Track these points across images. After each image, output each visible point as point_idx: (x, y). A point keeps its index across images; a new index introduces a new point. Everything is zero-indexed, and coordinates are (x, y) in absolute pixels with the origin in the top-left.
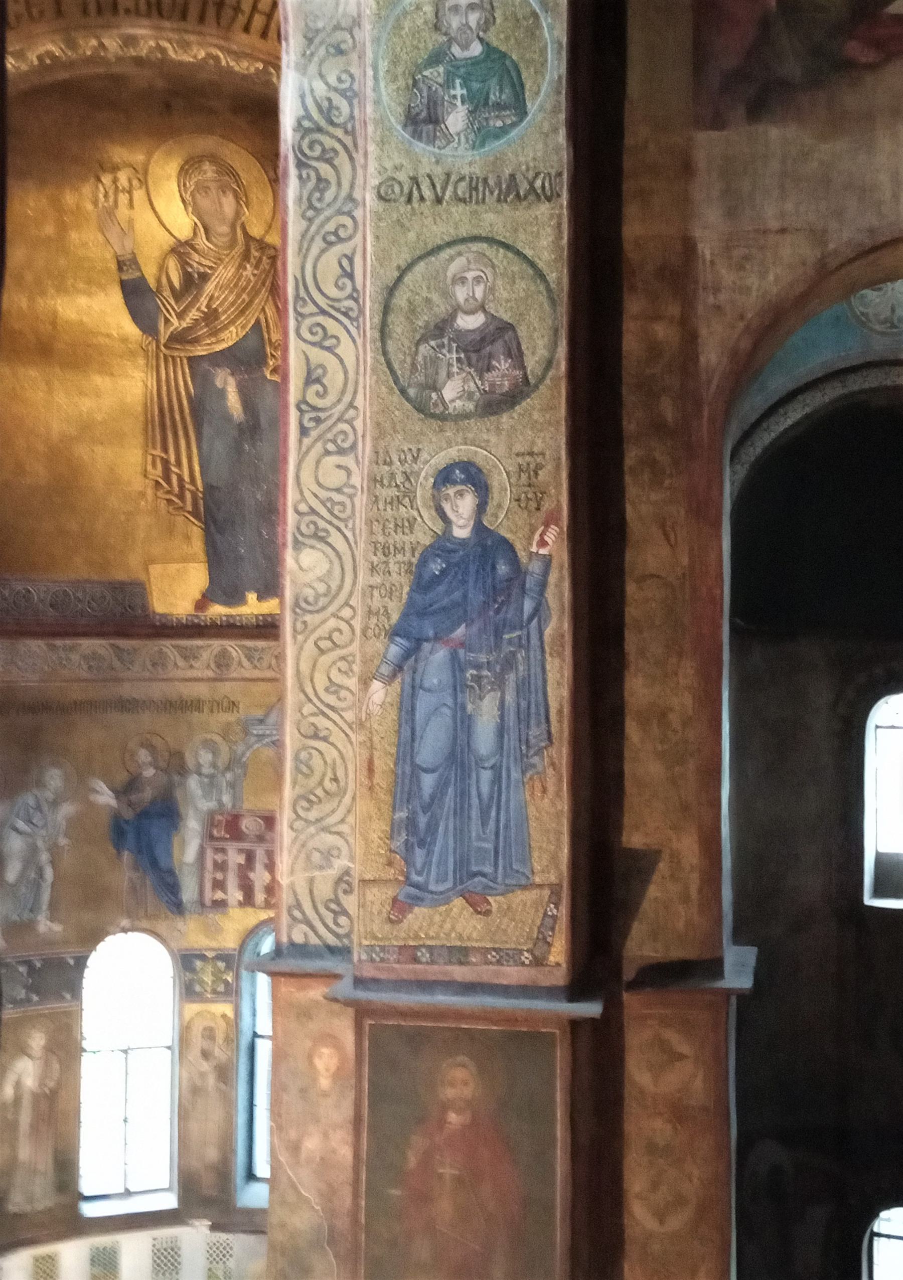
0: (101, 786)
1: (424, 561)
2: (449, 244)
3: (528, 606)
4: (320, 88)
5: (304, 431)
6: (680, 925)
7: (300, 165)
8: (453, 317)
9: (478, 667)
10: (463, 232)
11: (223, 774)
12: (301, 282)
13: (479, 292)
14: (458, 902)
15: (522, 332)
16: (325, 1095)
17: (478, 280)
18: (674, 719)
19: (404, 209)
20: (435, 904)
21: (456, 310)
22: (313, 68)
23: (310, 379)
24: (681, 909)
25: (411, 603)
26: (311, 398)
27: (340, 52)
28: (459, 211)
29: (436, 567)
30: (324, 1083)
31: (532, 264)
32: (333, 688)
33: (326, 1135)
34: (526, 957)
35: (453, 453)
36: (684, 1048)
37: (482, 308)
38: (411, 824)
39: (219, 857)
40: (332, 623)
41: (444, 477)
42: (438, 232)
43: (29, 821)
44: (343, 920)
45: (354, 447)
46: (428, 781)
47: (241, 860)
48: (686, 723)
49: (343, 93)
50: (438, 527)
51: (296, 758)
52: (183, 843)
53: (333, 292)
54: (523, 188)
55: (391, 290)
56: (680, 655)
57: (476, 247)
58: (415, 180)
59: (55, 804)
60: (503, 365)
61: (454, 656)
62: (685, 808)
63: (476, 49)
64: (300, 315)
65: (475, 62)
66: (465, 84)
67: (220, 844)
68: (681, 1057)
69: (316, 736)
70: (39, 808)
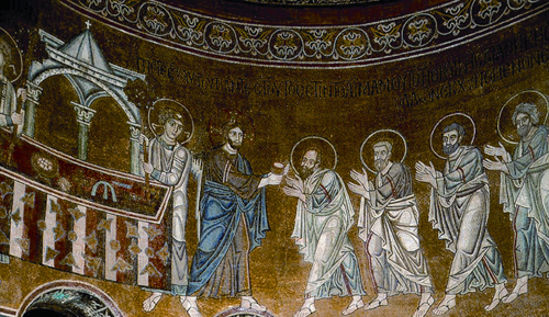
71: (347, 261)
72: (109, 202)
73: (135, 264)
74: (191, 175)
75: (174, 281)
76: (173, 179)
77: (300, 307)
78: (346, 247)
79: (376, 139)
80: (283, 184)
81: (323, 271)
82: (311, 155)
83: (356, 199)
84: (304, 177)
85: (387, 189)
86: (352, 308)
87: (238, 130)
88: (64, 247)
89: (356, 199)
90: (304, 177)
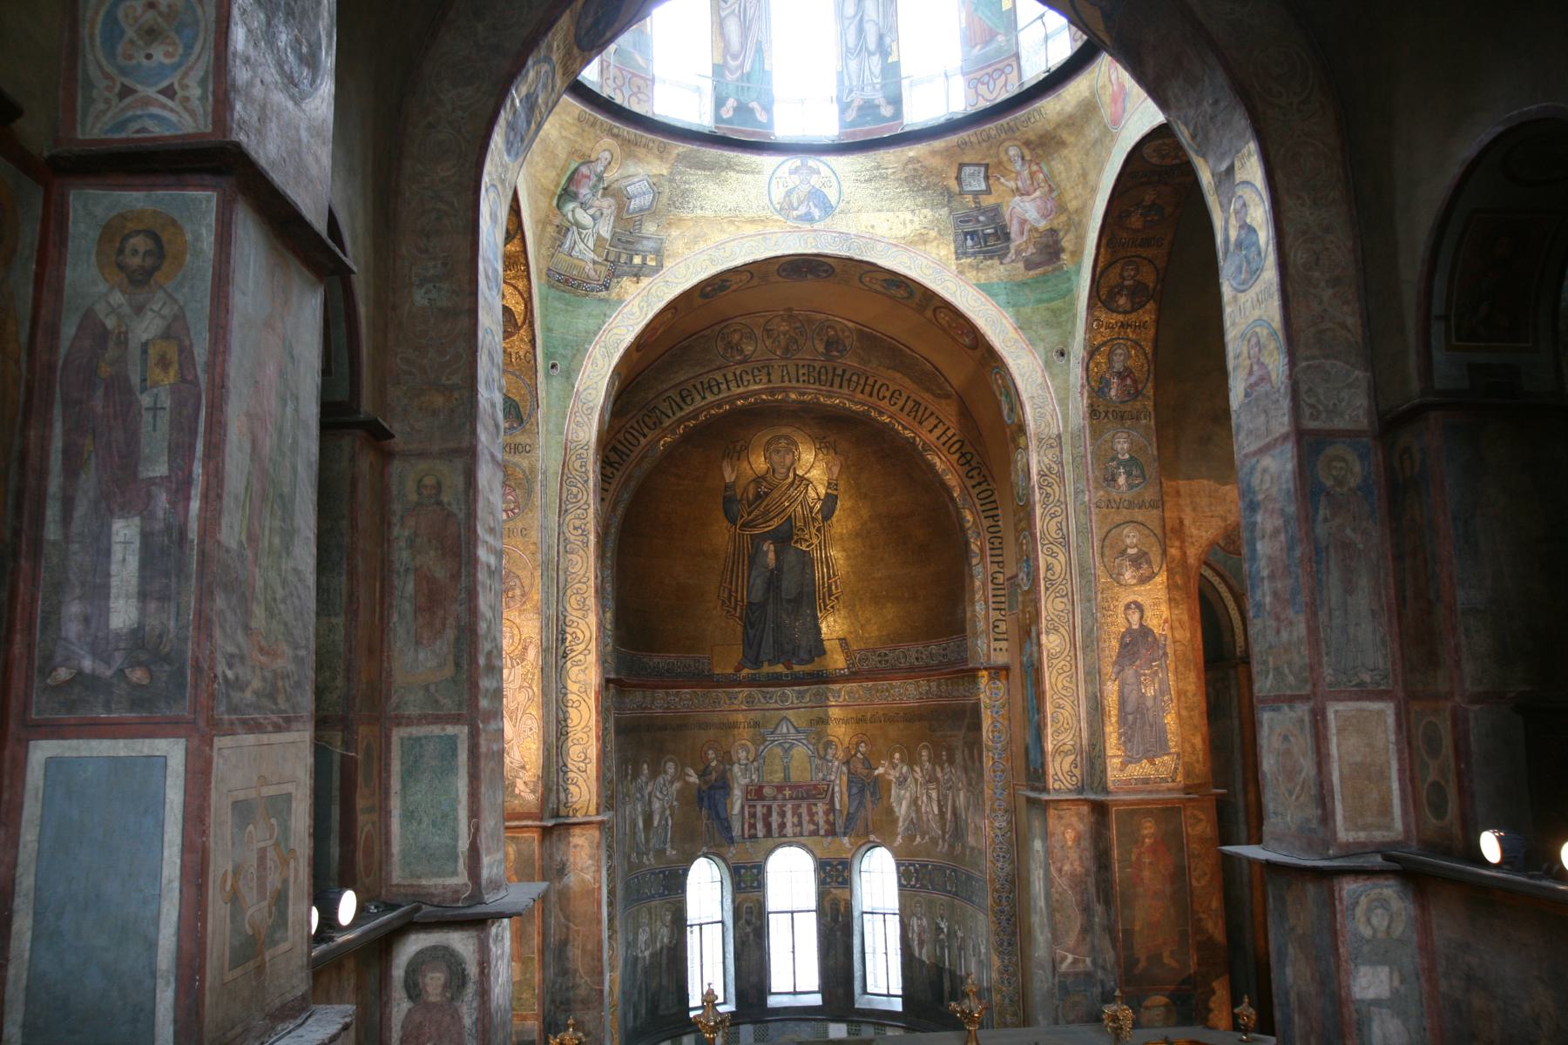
0: (691, 772)
1: (1123, 638)
2: (1124, 523)
3: (1161, 652)
4: (1046, 461)
5: (1047, 589)
6: (1197, 771)
7: (1040, 488)
8: (1125, 550)
9: (1145, 675)
10: (1128, 519)
11: (752, 762)
12: (1042, 532)
13: (1135, 540)
14: (1145, 761)
15: (1151, 555)
16: (1070, 848)
17: (1134, 536)
18: (1189, 694)
19: (1105, 510)
20: (1136, 763)
21: (1127, 547)
22: (1042, 453)
23: (1049, 568)
24: (1196, 765)
25: (1119, 652)
26: (1049, 575)
27: (1052, 447)
28: (1125, 511)
29: (1128, 640)
30: (1070, 843)
31: (1152, 531)
32: (1065, 688)
33: (1072, 864)
34: (1170, 780)
35: (1131, 598)
36: (1202, 817)
37: (1136, 546)
38: (1125, 733)
39: (752, 810)
40: (1063, 663)
41: (1128, 607)
42: (1118, 519)
43: (661, 792)
44: (1074, 778)
45: (1067, 594)
46: (1130, 718)
47: (765, 811)
48: (1194, 695)
49: (1054, 462)
50: (1127, 625)
51: (1052, 717)
52: (732, 804)
53: (1055, 536)
54: (1147, 504)
55: (1104, 540)
56: (1190, 670)
57: (1132, 525)
58: (1109, 501)
59: (672, 782)
60: (1145, 566)
61: (1136, 671)
62: (1196, 727)
63: (1127, 456)
64: (1043, 545)
65: (1127, 461)
66: (1124, 468)
67: (752, 803)
68: (1201, 820)
69: (1059, 707)
70: (665, 785)
71: (914, 815)
72: (803, 798)
73: (817, 825)
74: (842, 773)
75: (838, 830)
76: (833, 778)
77: (895, 841)
78: (913, 808)
79: (927, 747)
80: (886, 772)
81: (904, 821)
82: (897, 755)
83: (916, 780)
84: (894, 768)
85: (927, 777)
86: (916, 843)
87: (863, 745)
88: (782, 826)
89: (916, 780)
90: (894, 768)
